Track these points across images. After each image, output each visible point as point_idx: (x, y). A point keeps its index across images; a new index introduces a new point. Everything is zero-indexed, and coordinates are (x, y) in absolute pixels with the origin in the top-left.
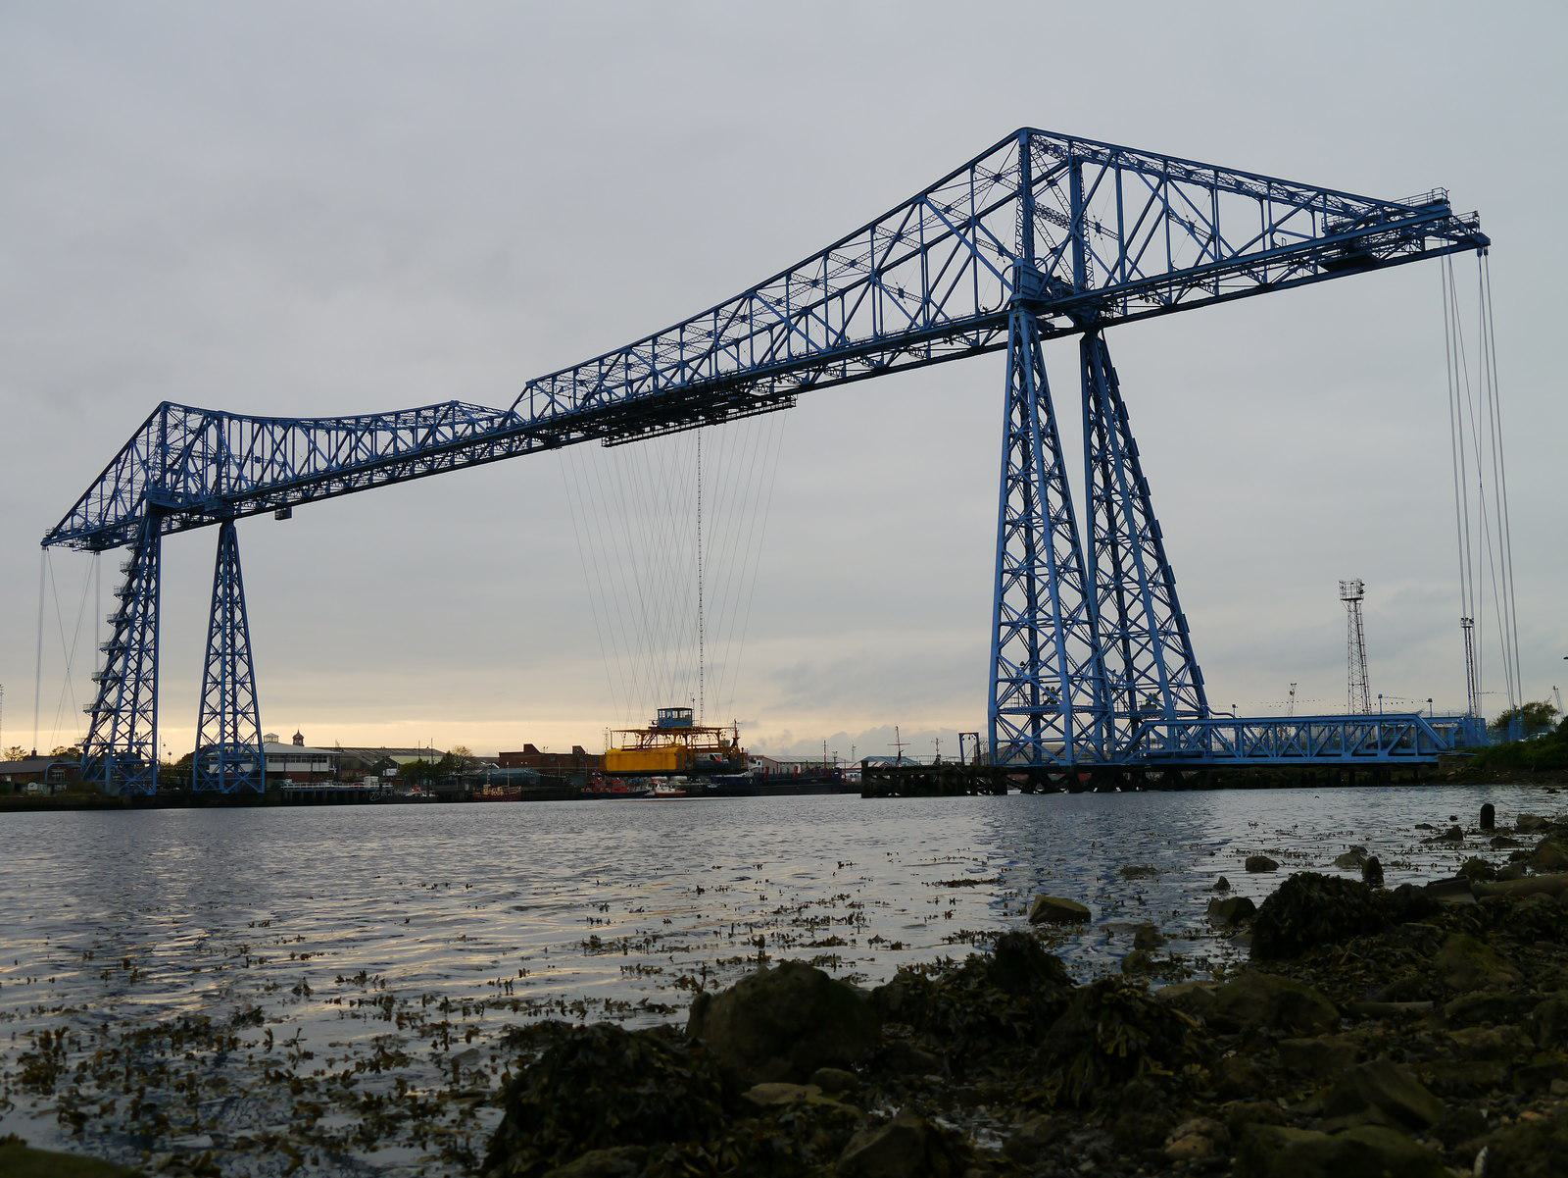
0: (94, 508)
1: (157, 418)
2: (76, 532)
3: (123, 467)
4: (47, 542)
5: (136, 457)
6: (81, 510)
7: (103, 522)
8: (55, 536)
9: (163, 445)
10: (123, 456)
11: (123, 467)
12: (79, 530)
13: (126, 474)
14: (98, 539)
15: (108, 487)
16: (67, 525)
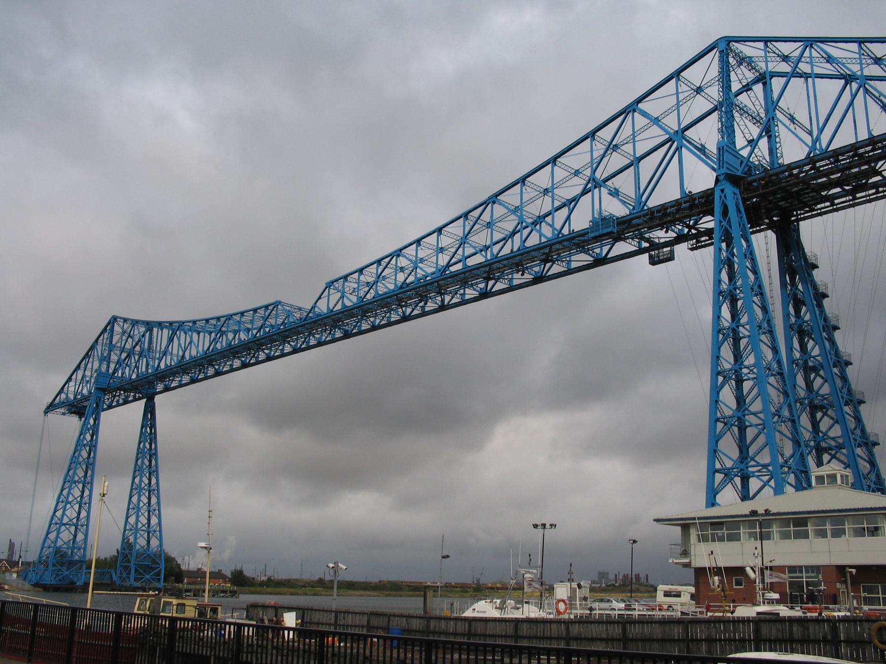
0: (72, 389)
1: (108, 328)
2: (62, 404)
3: (88, 363)
4: (46, 412)
5: (96, 354)
6: (65, 389)
7: (75, 397)
8: (51, 407)
9: (111, 347)
10: (89, 354)
11: (88, 363)
12: (63, 403)
13: (89, 366)
14: (77, 408)
15: (80, 373)
16: (57, 400)
